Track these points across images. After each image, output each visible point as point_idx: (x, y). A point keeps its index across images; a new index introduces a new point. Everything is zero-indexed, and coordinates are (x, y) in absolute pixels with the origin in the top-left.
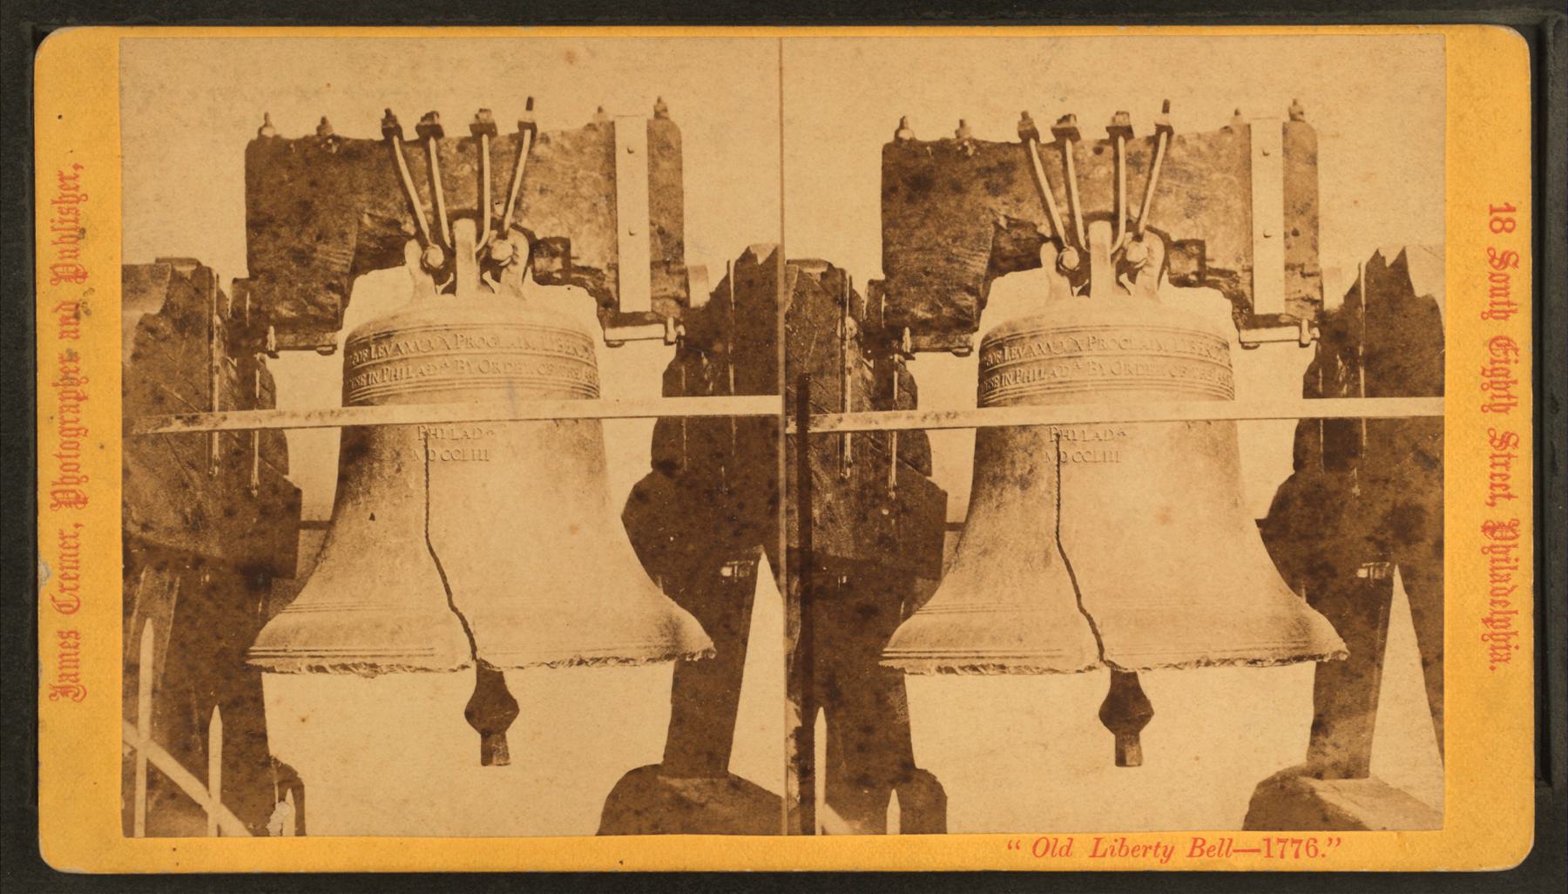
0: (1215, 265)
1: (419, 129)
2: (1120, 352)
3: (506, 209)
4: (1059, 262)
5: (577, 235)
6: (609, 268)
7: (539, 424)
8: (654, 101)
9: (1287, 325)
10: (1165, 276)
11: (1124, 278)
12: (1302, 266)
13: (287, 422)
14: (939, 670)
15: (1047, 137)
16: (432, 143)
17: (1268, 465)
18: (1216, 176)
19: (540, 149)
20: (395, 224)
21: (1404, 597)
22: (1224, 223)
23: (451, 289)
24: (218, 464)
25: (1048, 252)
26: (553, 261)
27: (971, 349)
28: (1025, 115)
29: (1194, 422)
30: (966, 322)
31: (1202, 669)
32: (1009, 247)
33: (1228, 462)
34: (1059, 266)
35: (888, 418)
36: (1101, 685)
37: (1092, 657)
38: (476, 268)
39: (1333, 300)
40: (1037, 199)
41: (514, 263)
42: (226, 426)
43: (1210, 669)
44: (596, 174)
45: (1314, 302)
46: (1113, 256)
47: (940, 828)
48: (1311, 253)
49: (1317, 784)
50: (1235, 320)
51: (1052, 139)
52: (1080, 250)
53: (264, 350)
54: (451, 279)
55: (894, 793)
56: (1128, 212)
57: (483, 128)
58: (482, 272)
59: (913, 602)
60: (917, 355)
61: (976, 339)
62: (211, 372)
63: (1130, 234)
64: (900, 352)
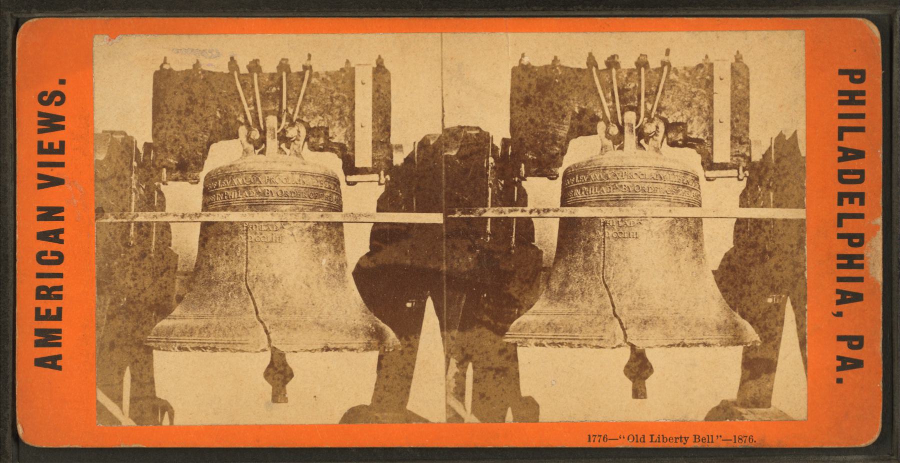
2: (639, 180)
3: (294, 113)
4: (607, 132)
8: (377, 57)
9: (731, 168)
12: (740, 138)
14: (536, 345)
15: (602, 66)
16: (255, 75)
17: (719, 241)
19: (314, 80)
22: (699, 115)
23: (263, 152)
26: (318, 139)
27: (558, 176)
30: (556, 160)
35: (511, 211)
36: (625, 354)
37: (620, 341)
38: (276, 142)
42: (138, 219)
45: (743, 156)
46: (637, 130)
48: (745, 131)
50: (703, 164)
51: (605, 67)
52: (617, 124)
53: (160, 180)
54: (263, 146)
56: (646, 106)
57: (283, 66)
58: (279, 145)
60: (528, 178)
63: (646, 119)
64: (519, 177)
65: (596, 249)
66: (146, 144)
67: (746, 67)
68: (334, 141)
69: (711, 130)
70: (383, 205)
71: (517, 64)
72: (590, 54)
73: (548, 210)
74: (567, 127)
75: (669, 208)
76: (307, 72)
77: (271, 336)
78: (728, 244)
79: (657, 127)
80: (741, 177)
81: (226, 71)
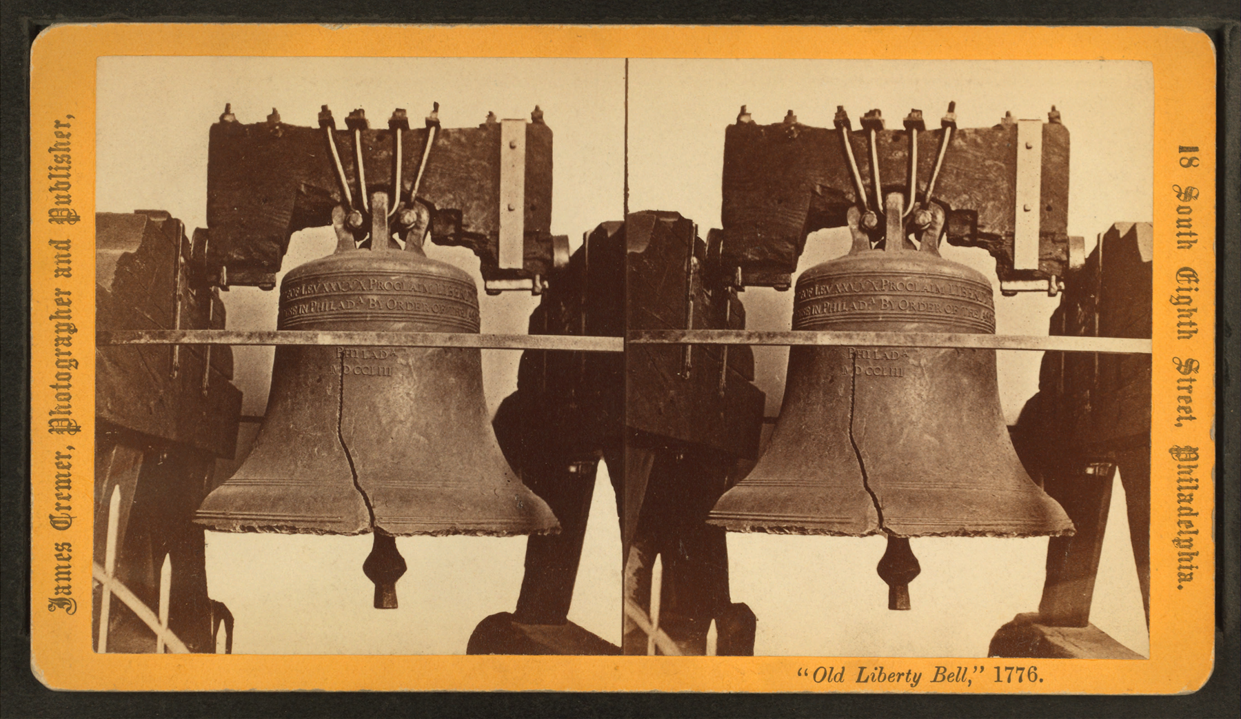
0: (985, 231)
1: (347, 121)
5: (468, 209)
6: (491, 234)
7: (430, 350)
8: (533, 109)
10: (945, 237)
11: (912, 237)
12: (1054, 234)
13: (234, 340)
14: (753, 529)
15: (856, 126)
17: (1018, 383)
18: (988, 163)
19: (441, 142)
20: (328, 194)
21: (1123, 492)
22: (993, 199)
23: (367, 245)
24: (177, 369)
25: (853, 215)
26: (449, 228)
27: (789, 285)
28: (840, 109)
29: (963, 349)
31: (959, 538)
32: (822, 209)
33: (987, 381)
34: (862, 228)
35: (720, 335)
36: (879, 545)
39: (1077, 259)
40: (846, 172)
41: (418, 228)
42: (185, 340)
43: (966, 538)
44: (484, 163)
45: (1060, 261)
46: (904, 220)
47: (750, 652)
48: (1060, 225)
49: (1046, 630)
50: (998, 271)
51: (861, 128)
55: (713, 622)
57: (399, 120)
58: (391, 234)
59: (737, 476)
60: (746, 288)
61: (794, 277)
62: (174, 300)
65: (841, 392)
66: (198, 231)
67: (1065, 130)
68: (471, 230)
69: (1012, 221)
70: (539, 324)
71: (734, 122)
72: (840, 109)
73: (775, 335)
74: (804, 215)
75: (947, 335)
76: (433, 130)
77: (375, 511)
78: (1033, 389)
79: (934, 216)
80: (1053, 291)
81: (316, 125)
